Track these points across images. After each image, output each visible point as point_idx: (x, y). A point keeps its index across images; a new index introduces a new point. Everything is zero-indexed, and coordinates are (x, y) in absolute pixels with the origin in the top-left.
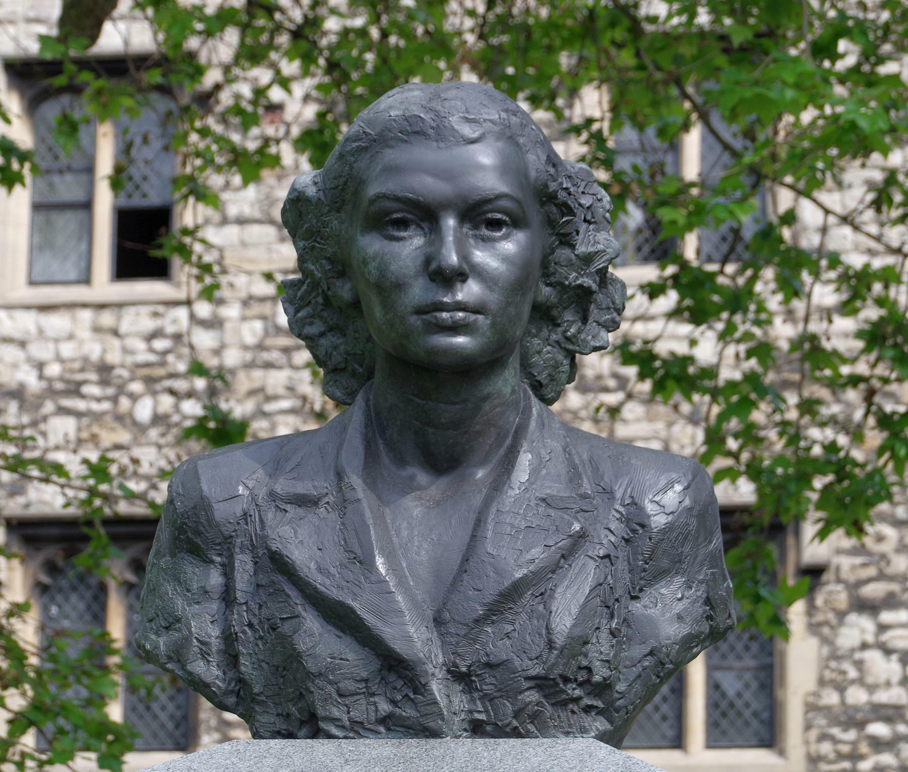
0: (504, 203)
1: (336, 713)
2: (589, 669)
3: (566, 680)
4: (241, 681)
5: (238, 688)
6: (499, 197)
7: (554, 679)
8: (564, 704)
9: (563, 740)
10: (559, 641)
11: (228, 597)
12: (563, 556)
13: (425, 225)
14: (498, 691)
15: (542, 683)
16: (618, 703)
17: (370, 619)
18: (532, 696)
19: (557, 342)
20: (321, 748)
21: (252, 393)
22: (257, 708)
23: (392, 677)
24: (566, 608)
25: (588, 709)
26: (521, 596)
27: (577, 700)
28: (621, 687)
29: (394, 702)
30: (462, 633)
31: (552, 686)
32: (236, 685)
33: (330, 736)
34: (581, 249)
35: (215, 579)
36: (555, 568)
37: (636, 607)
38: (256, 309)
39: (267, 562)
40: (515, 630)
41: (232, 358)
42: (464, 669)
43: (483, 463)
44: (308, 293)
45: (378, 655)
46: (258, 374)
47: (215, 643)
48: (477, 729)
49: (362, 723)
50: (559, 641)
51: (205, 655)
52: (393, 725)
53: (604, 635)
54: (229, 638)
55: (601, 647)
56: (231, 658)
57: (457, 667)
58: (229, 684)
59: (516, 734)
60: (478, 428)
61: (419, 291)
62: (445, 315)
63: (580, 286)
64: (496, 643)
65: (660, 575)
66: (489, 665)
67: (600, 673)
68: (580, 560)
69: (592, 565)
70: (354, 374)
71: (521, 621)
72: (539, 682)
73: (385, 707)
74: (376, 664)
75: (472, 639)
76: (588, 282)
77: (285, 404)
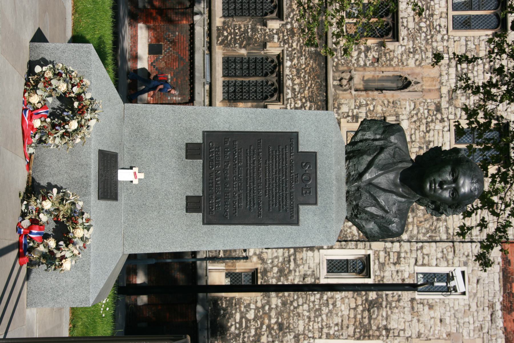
0: (457, 196)
1: (351, 164)
3: (358, 210)
8: (353, 209)
10: (366, 209)
11: (375, 140)
15: (357, 205)
18: (354, 203)
21: (426, 49)
24: (372, 210)
25: (352, 214)
27: (354, 212)
28: (357, 220)
29: (353, 175)
34: (448, 209)
35: (378, 137)
37: (373, 223)
38: (446, 49)
41: (435, 44)
43: (402, 190)
45: (362, 172)
46: (431, 50)
47: (365, 137)
48: (348, 192)
50: (366, 209)
52: (349, 176)
54: (366, 140)
56: (361, 141)
62: (433, 185)
64: (365, 196)
65: (380, 227)
66: (360, 195)
71: (370, 200)
76: (441, 211)
77: (424, 57)
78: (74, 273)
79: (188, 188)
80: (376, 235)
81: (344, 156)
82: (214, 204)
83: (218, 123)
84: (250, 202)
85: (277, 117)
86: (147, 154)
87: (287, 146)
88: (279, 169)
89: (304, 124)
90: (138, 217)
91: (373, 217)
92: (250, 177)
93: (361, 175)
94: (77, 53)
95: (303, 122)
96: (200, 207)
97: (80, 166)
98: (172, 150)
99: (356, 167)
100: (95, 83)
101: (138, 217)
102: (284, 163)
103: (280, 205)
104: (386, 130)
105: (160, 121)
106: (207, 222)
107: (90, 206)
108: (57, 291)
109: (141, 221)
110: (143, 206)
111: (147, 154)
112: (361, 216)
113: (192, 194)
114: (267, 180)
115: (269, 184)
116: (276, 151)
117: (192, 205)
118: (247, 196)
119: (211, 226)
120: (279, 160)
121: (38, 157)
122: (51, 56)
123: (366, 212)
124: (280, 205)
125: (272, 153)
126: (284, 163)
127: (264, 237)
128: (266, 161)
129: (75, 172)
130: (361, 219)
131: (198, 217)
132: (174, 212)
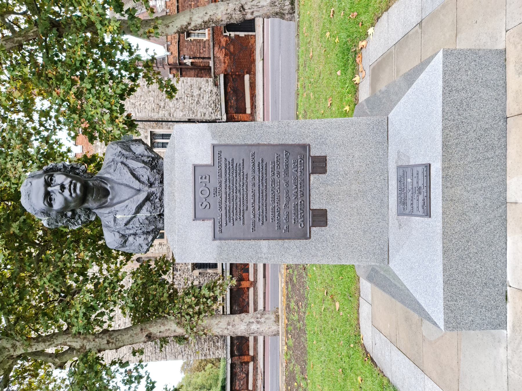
0: (46, 177)
1: (159, 210)
2: (149, 161)
3: (151, 165)
4: (152, 231)
6: (45, 178)
8: (156, 166)
9: (164, 166)
17: (139, 203)
18: (155, 171)
20: (165, 213)
27: (156, 163)
28: (153, 156)
33: (163, 211)
35: (132, 237)
36: (128, 167)
39: (127, 226)
44: (72, 223)
47: (145, 236)
48: (162, 182)
51: (147, 239)
53: (142, 158)
54: (143, 233)
55: (146, 159)
56: (148, 233)
59: (163, 174)
61: (67, 193)
66: (149, 179)
67: (150, 159)
68: (127, 163)
69: (128, 161)
70: (90, 213)
73: (157, 200)
78: (459, 85)
79: (324, 181)
81: (165, 217)
82: (299, 165)
83: (295, 247)
84: (262, 168)
85: (235, 254)
86: (366, 215)
87: (225, 225)
88: (233, 201)
89: (207, 249)
90: (374, 152)
91: (137, 158)
92: (262, 193)
93: (148, 199)
94: (459, 321)
95: (208, 251)
96: (313, 162)
97: (454, 198)
98: (341, 219)
99: (153, 206)
100: (437, 289)
101: (374, 152)
102: (228, 208)
103: (232, 165)
105: (353, 248)
106: (305, 147)
107: (443, 156)
108: (476, 65)
109: (371, 148)
110: (369, 163)
111: (366, 215)
112: (149, 159)
113: (320, 175)
114: (245, 190)
115: (243, 186)
116: (236, 220)
117: (320, 165)
118: (266, 174)
119: (302, 142)
120: (233, 211)
121: (497, 208)
122: (486, 316)
123: (143, 162)
124: (232, 165)
125: (240, 218)
126: (228, 208)
127: (249, 133)
128: (247, 209)
129: (459, 192)
130: (148, 157)
131: (315, 152)
132: (338, 158)
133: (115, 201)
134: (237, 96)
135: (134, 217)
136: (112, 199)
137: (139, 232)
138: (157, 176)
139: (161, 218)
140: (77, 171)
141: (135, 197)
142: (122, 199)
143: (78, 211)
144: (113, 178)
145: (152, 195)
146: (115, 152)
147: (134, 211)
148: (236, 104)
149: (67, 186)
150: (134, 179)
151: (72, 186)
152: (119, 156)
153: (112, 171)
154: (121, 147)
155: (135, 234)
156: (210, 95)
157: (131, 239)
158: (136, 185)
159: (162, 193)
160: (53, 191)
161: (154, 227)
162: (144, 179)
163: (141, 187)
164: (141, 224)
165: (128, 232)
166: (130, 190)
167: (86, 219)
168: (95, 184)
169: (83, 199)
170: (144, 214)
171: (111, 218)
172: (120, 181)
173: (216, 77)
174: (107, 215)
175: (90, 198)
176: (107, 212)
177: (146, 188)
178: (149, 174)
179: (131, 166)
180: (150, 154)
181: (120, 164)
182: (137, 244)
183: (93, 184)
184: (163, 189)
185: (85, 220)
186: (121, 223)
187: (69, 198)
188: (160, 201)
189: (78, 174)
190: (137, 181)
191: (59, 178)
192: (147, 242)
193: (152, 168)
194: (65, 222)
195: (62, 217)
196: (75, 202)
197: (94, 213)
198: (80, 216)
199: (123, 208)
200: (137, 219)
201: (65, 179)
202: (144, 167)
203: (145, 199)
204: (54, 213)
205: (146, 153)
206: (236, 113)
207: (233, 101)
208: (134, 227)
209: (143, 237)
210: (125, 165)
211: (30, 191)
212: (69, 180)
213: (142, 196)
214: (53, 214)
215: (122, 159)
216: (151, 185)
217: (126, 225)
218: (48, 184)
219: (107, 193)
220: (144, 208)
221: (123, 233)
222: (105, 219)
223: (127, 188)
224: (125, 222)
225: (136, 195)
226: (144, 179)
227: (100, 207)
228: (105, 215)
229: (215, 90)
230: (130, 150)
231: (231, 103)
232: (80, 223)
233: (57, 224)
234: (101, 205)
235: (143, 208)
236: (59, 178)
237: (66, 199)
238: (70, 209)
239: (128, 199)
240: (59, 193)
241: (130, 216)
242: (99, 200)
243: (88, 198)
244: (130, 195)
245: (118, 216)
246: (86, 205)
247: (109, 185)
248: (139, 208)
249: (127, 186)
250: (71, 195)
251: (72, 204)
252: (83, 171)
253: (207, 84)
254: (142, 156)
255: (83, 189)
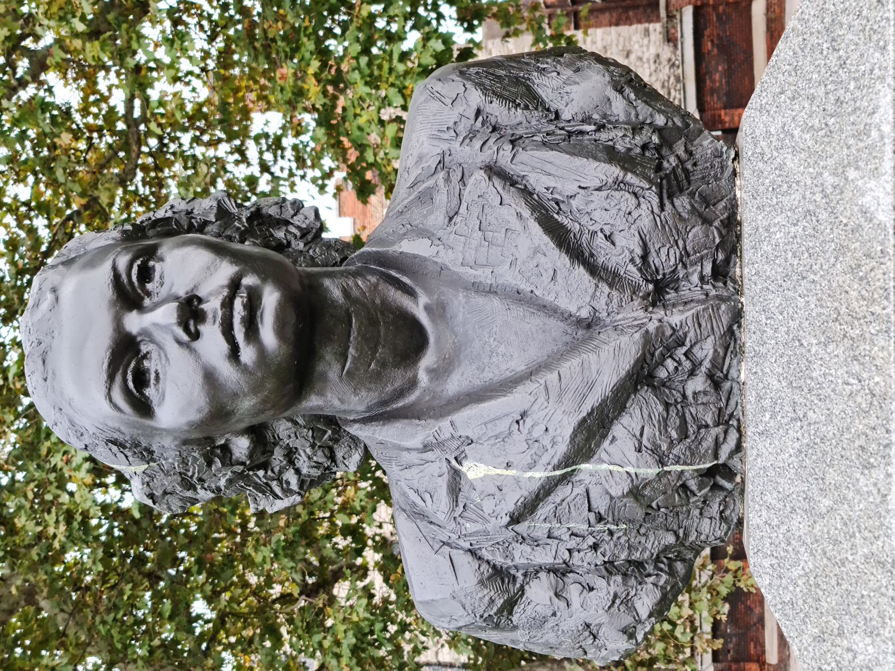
0: (123, 262)
2: (645, 147)
3: (659, 168)
5: (665, 560)
6: (114, 268)
7: (662, 179)
12: (512, 185)
13: (144, 349)
14: (676, 242)
16: (679, 124)
17: (593, 400)
18: (682, 203)
19: (305, 245)
22: (692, 538)
23: (662, 374)
26: (562, 226)
28: (660, 120)
30: (607, 289)
31: (669, 182)
32: (662, 562)
36: (527, 193)
37: (566, 115)
40: (602, 230)
42: (651, 287)
49: (720, 409)
53: (603, 136)
54: (609, 568)
56: (635, 569)
57: (649, 294)
58: (661, 570)
60: (378, 301)
63: (248, 219)
66: (645, 257)
68: (515, 169)
69: (522, 156)
72: (665, 196)
73: (698, 384)
74: (645, 393)
75: (614, 279)
80: (548, 64)
99: (674, 420)
104: (500, 611)
112: (639, 140)
123: (611, 155)
133: (454, 385)
134: (730, 61)
135: (564, 479)
136: (436, 373)
137: (584, 560)
138: (697, 231)
139: (716, 487)
140: (280, 234)
141: (570, 366)
142: (490, 375)
143: (283, 428)
144: (446, 257)
145: (669, 351)
146: (450, 116)
147: (562, 448)
148: (728, 83)
149: (213, 306)
150: (563, 260)
151: (238, 304)
152: (472, 135)
153: (436, 219)
154: (485, 90)
155: (561, 571)
156: (653, 67)
157: (539, 593)
158: (576, 291)
159: (730, 340)
160: (145, 332)
161: (670, 539)
162: (620, 254)
163: (601, 304)
164: (600, 519)
165: (522, 555)
166: (536, 322)
167: (318, 465)
168: (355, 293)
169: (296, 374)
170: (619, 463)
171: (433, 474)
172: (484, 276)
173: (670, 17)
174: (414, 457)
175: (331, 368)
176: (416, 442)
177: (634, 312)
178: (646, 222)
179: (538, 182)
180: (644, 111)
181: (481, 175)
182: (571, 621)
183: (346, 293)
184: (737, 315)
185: (316, 473)
186: (488, 506)
187: (226, 371)
188: (716, 385)
189: (281, 247)
190: (581, 271)
191: (187, 267)
192: (627, 620)
193: (670, 186)
194: (222, 483)
195: (210, 463)
196: (255, 389)
197: (355, 440)
198: (290, 455)
199: (503, 426)
200: (579, 490)
201: (209, 270)
202: (619, 184)
203: (629, 375)
204: (168, 442)
205: (618, 107)
206: (725, 108)
207: (718, 77)
208: (561, 531)
209: (605, 589)
210: (510, 180)
211: (51, 333)
212: (226, 270)
213: (607, 363)
214: (168, 450)
215: (487, 156)
216: (660, 290)
217: (515, 519)
218: (129, 296)
219: (411, 340)
220: (625, 428)
221: (499, 560)
222: (407, 474)
223: (518, 311)
224: (510, 504)
225: (573, 348)
226: (620, 254)
227: (381, 414)
228: (407, 457)
229: (666, 52)
230: (533, 100)
231: (713, 81)
232: (294, 486)
233: (189, 494)
234: (384, 403)
235: (617, 430)
236: (187, 267)
237: (210, 377)
238: (243, 425)
239: (530, 375)
240: (179, 342)
241: (540, 475)
242: (377, 377)
243: (320, 367)
244: (534, 353)
245: (473, 471)
246: (313, 402)
247: (423, 299)
248: (593, 432)
249: (518, 297)
250: (234, 353)
251: (247, 404)
252: (304, 233)
253: (646, 41)
254: (600, 127)
255: (292, 319)
